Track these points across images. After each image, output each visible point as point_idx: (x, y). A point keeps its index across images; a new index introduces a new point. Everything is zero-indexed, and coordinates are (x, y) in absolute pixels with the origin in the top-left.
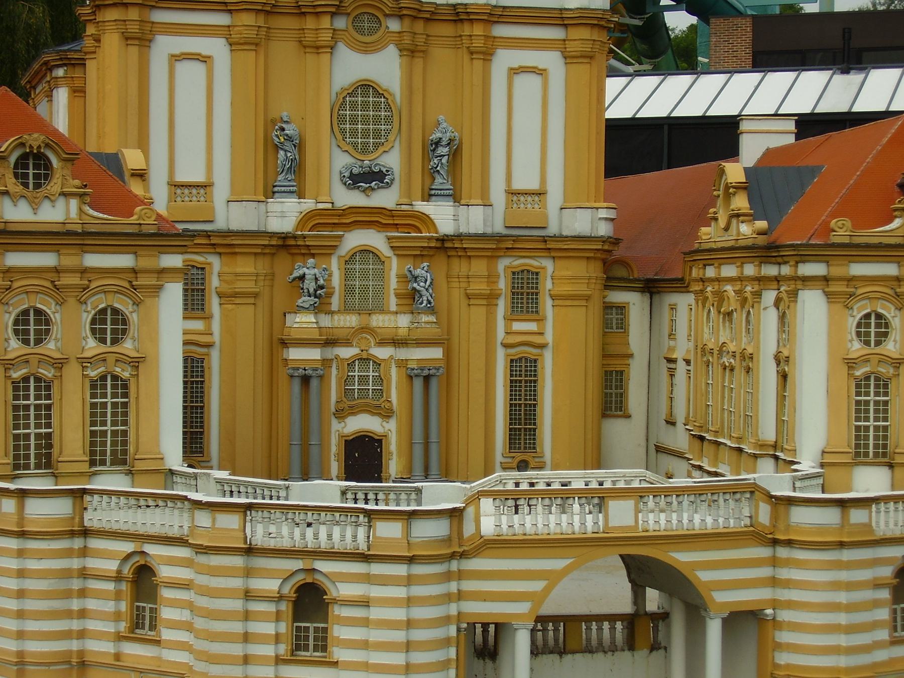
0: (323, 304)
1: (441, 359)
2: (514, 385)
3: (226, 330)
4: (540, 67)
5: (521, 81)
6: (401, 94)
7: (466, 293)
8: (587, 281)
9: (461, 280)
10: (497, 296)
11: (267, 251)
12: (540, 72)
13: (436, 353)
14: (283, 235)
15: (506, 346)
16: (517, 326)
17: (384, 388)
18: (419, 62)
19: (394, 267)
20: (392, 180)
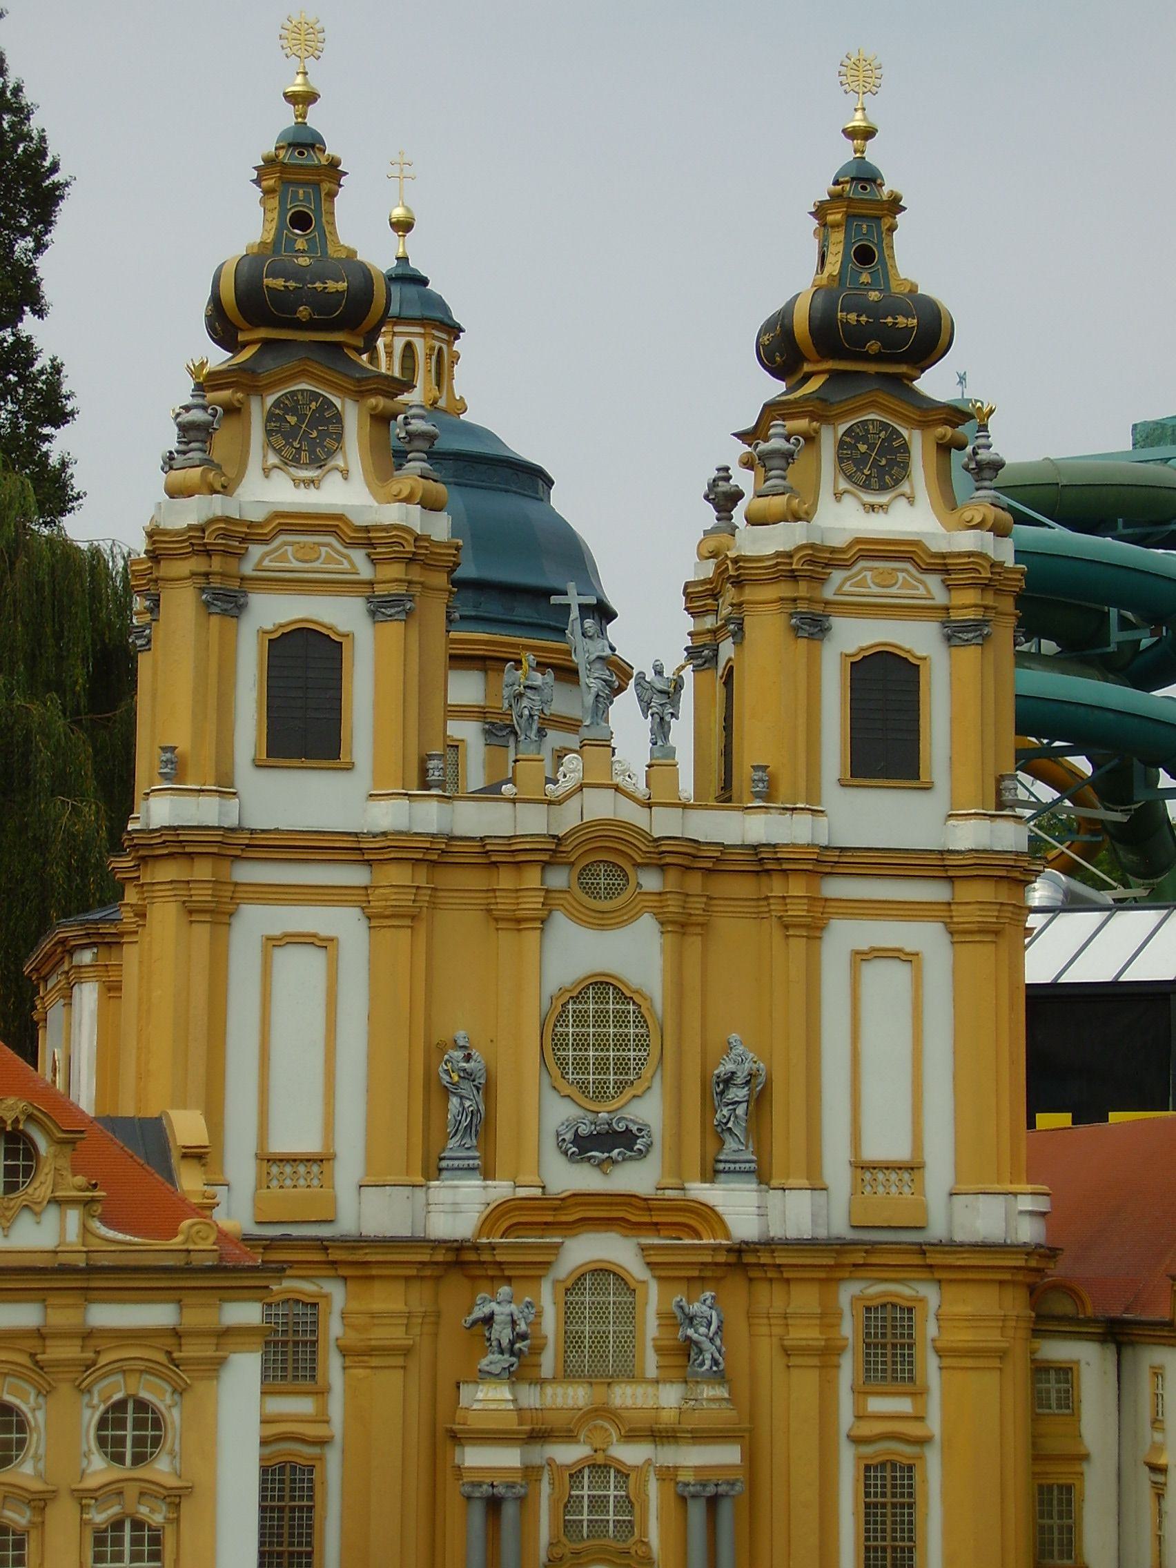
0: (525, 1366)
1: (738, 1466)
2: (871, 1512)
3: (355, 1414)
4: (908, 949)
5: (873, 973)
6: (664, 997)
7: (782, 1346)
8: (1000, 1324)
9: (772, 1321)
10: (839, 1351)
11: (428, 1272)
12: (908, 957)
13: (729, 1455)
14: (455, 1244)
15: (856, 1440)
16: (877, 1405)
17: (636, 1518)
18: (694, 944)
19: (653, 1299)
20: (649, 1146)
